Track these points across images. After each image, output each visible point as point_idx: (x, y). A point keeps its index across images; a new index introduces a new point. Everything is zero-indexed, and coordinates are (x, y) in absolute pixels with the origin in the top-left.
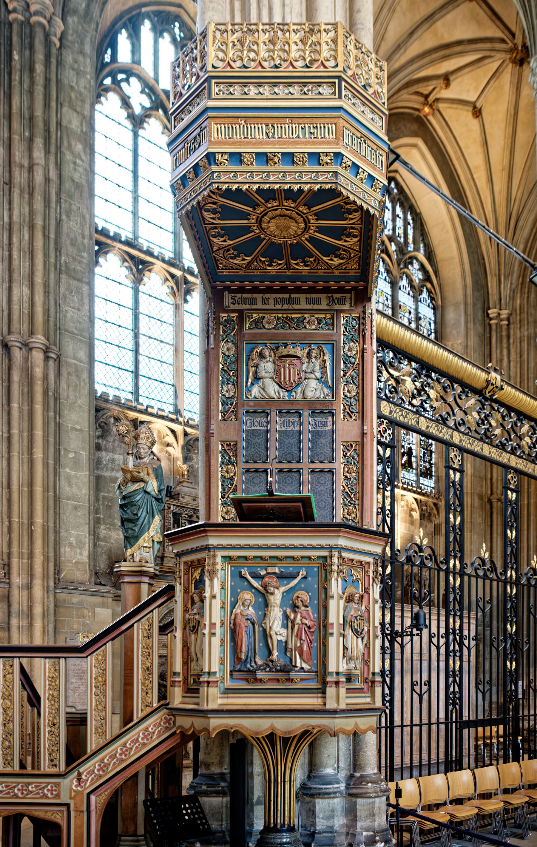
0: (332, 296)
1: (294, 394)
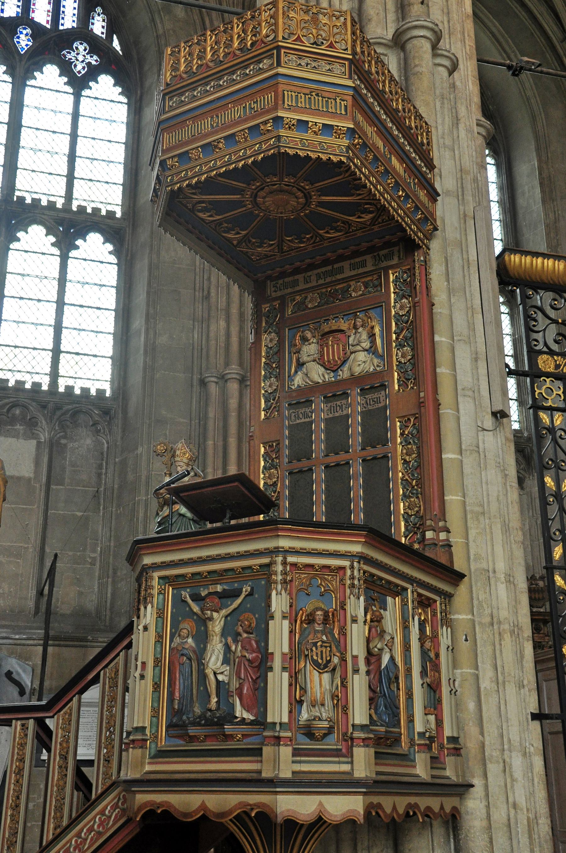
0: (378, 255)
1: (341, 372)
